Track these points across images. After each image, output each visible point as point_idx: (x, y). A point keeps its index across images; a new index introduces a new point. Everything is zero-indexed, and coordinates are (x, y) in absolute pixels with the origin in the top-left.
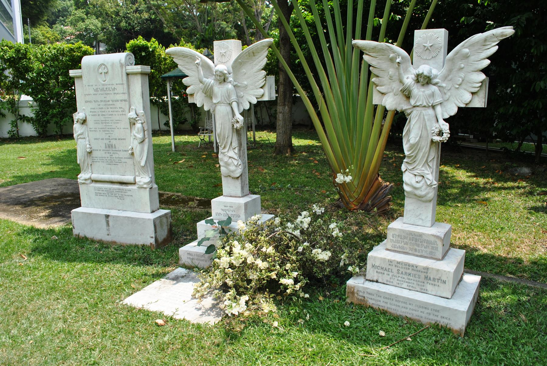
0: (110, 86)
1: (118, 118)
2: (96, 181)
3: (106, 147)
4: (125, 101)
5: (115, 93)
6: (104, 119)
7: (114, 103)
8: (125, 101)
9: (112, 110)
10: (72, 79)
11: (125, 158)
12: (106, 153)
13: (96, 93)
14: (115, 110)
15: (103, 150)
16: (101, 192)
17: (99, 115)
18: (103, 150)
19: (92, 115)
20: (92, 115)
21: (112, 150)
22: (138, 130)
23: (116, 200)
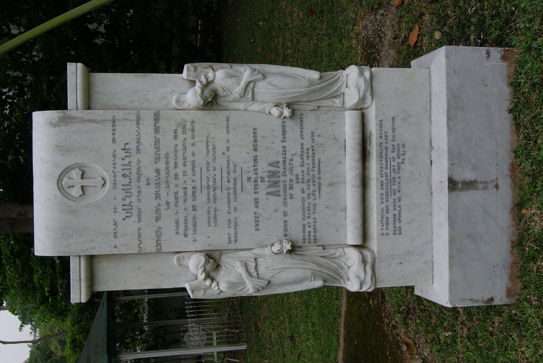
0: (119, 162)
1: (201, 148)
2: (365, 235)
3: (276, 194)
4: (157, 118)
5: (138, 150)
6: (205, 191)
7: (162, 153)
8: (157, 118)
9: (180, 162)
10: (95, 297)
11: (302, 136)
12: (292, 197)
13: (135, 212)
14: (180, 154)
15: (285, 204)
16: (391, 216)
17: (194, 208)
18: (285, 204)
19: (195, 231)
20: (195, 231)
21: (284, 175)
22: (231, 76)
23: (406, 168)
